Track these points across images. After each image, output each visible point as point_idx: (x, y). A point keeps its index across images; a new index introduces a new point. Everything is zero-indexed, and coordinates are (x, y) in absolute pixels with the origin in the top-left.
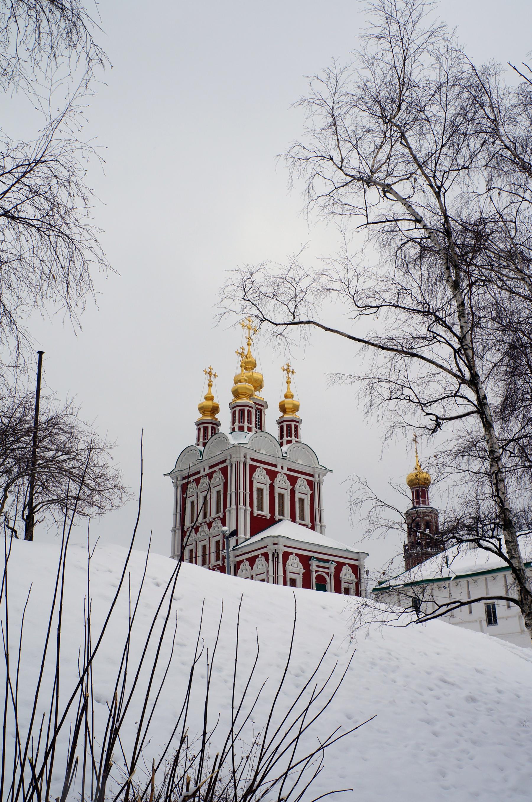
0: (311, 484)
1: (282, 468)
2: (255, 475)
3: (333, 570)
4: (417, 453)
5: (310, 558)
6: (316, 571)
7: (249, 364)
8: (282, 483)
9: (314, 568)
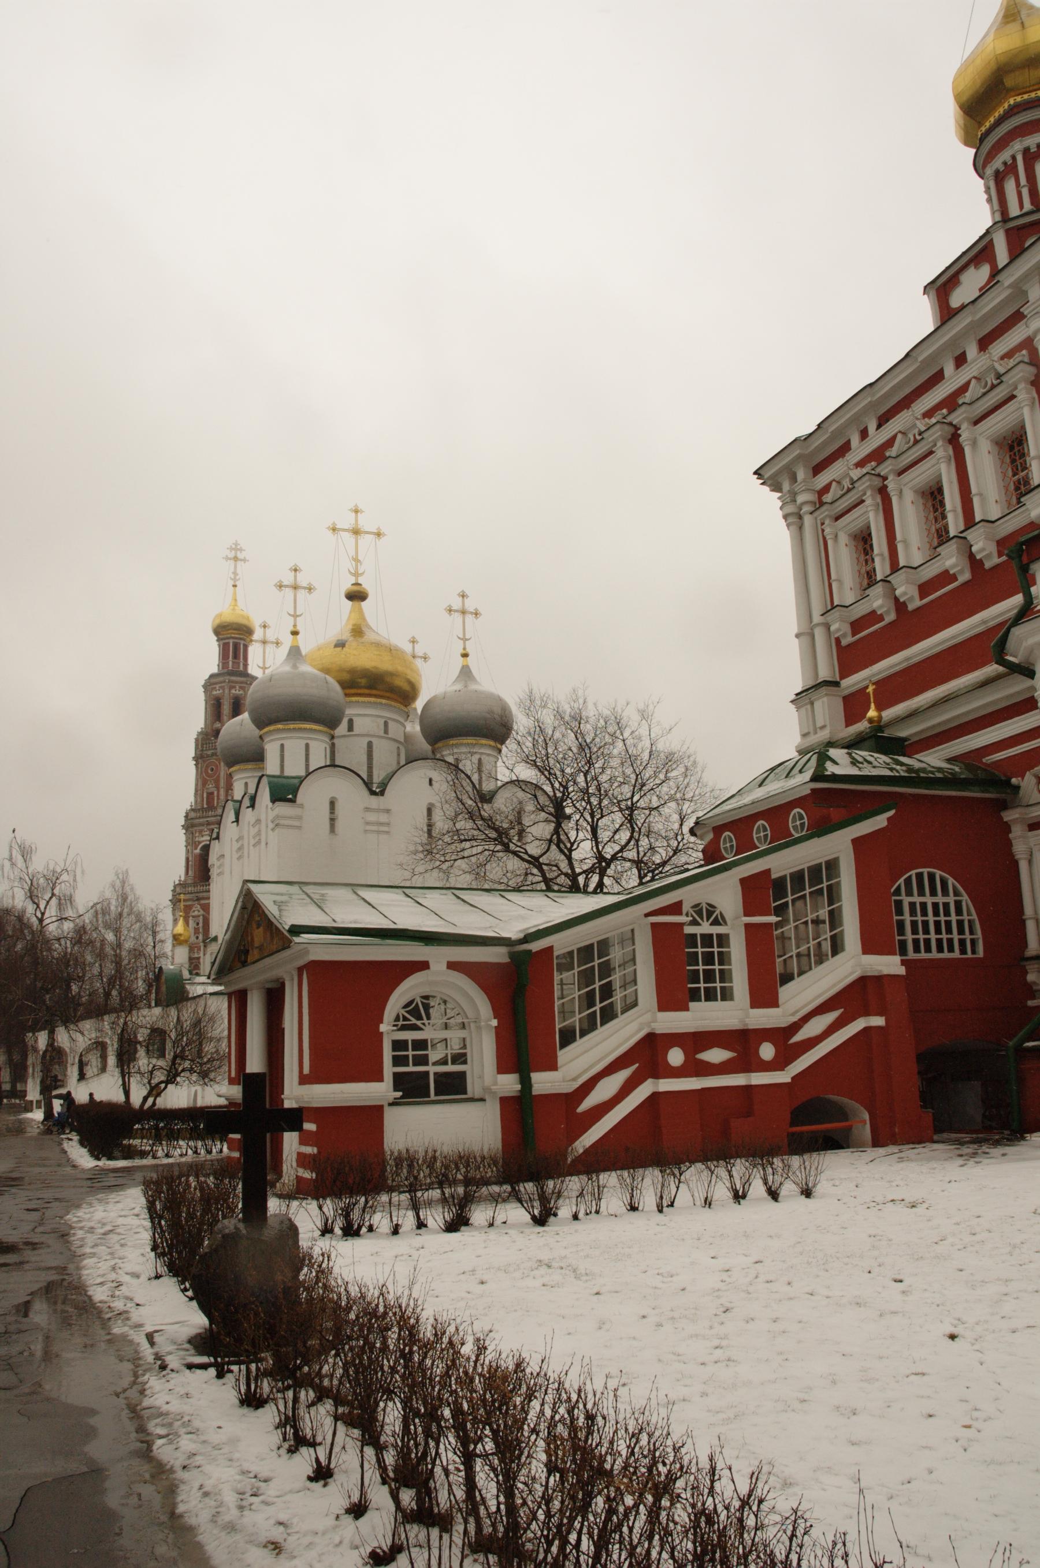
4: (235, 580)
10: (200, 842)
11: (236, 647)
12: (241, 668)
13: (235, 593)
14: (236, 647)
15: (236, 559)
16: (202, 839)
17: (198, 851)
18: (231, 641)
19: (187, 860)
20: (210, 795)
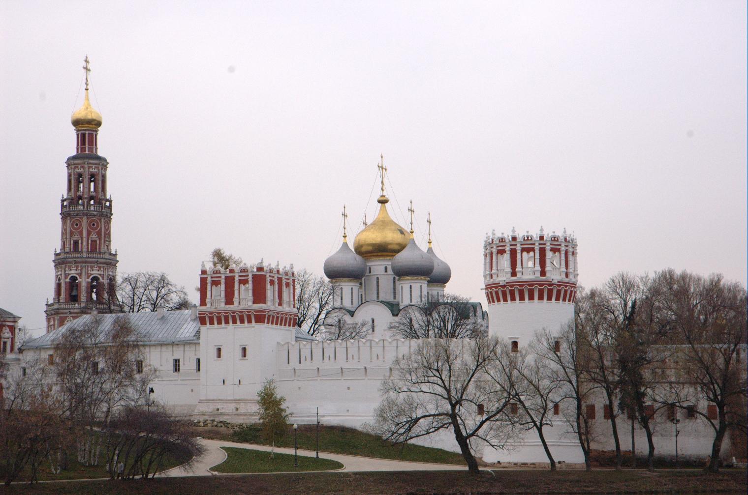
4: (87, 84)
10: (69, 274)
12: (94, 153)
14: (91, 135)
16: (70, 272)
17: (68, 280)
18: (87, 132)
19: (59, 286)
20: (76, 243)
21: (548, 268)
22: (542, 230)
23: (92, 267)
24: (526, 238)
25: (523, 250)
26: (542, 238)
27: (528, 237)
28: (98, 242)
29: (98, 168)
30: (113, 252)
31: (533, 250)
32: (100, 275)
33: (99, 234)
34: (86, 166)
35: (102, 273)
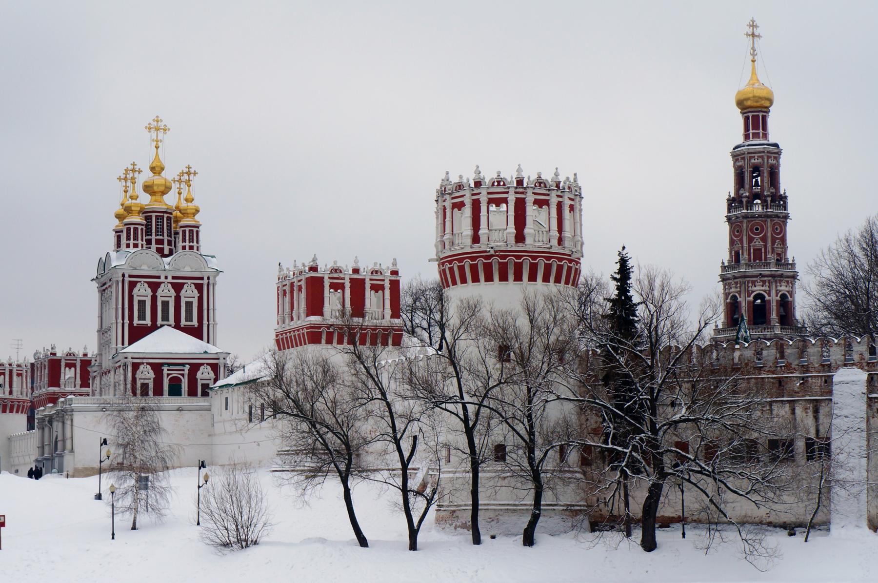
0: (199, 287)
1: (166, 278)
2: (135, 291)
3: (186, 372)
4: (753, 55)
5: (163, 364)
6: (168, 375)
7: (156, 169)
8: (166, 292)
9: (165, 372)
11: (756, 118)
13: (754, 69)
15: (753, 35)
18: (750, 115)
20: (737, 254)
21: (528, 231)
22: (519, 170)
23: (754, 283)
24: (496, 184)
25: (490, 201)
26: (520, 182)
27: (499, 182)
28: (763, 250)
29: (762, 157)
30: (790, 262)
31: (505, 201)
32: (765, 291)
33: (764, 239)
34: (746, 156)
35: (767, 288)
